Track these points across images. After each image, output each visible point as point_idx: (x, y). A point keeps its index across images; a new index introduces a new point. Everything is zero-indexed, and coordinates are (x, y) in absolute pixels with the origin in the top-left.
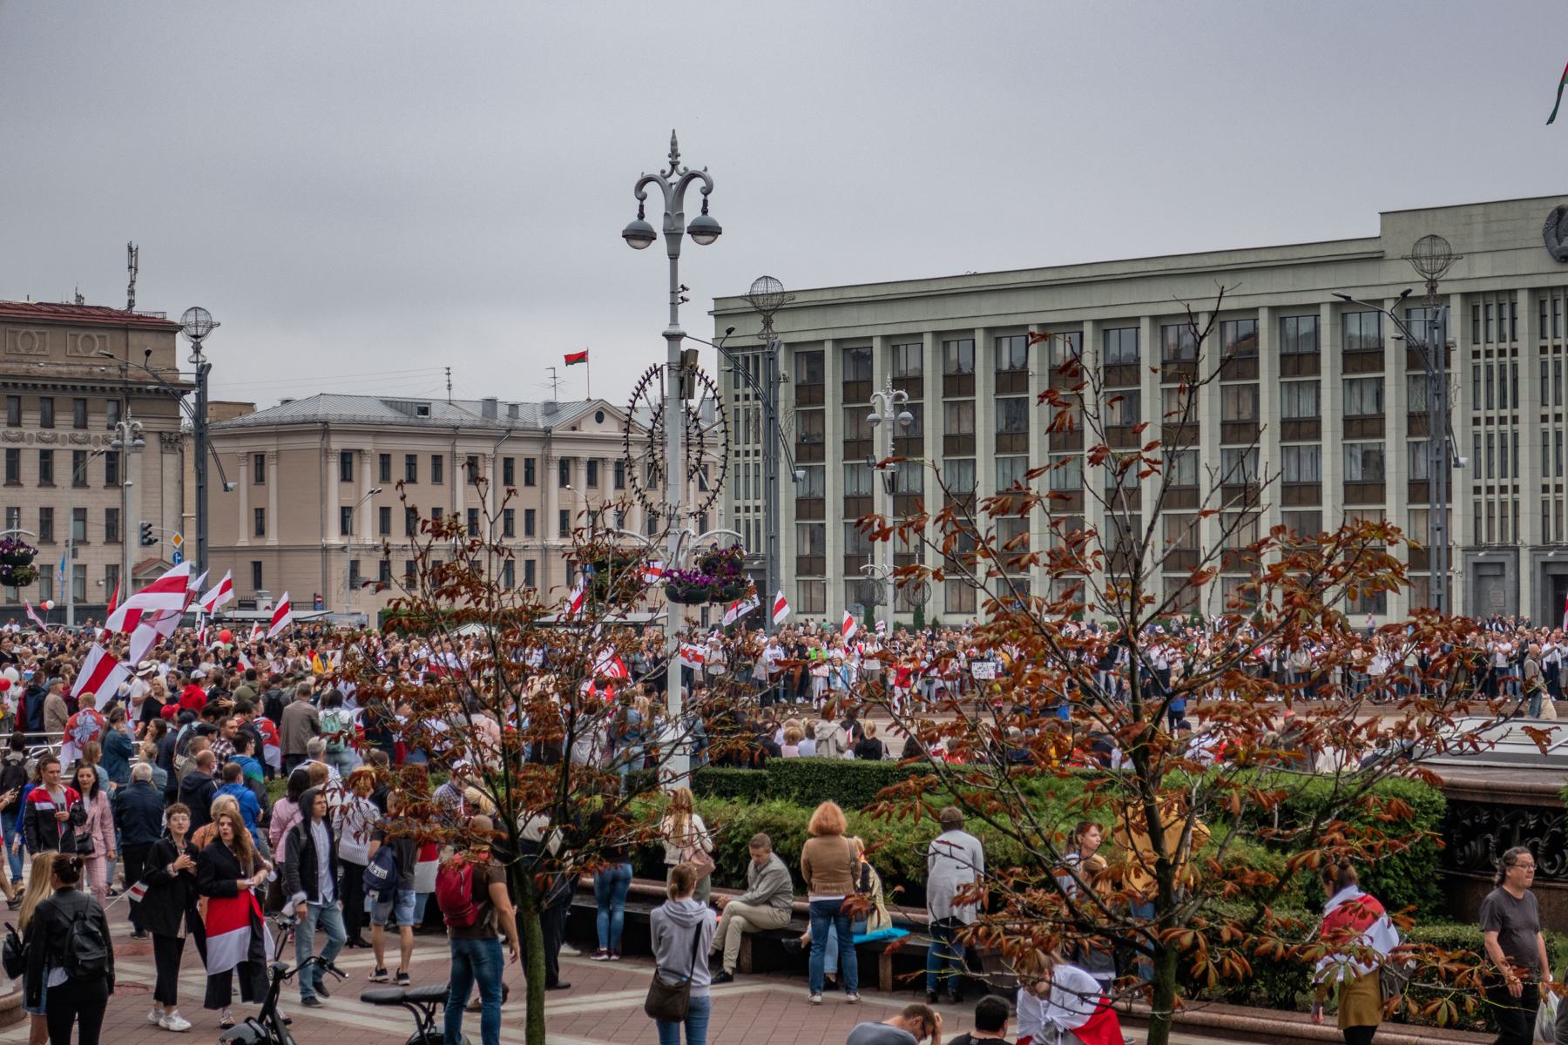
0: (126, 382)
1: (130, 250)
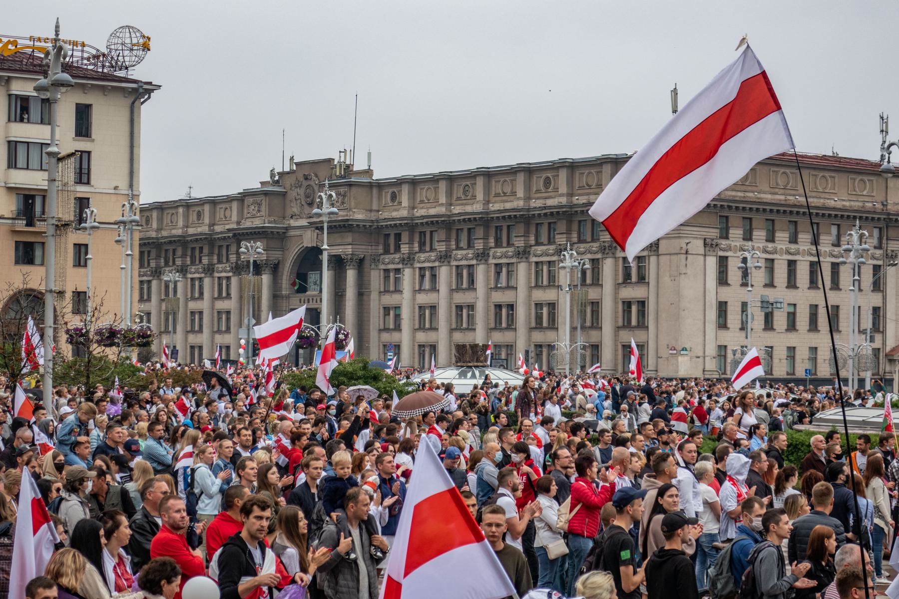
0: (889, 214)
1: (882, 118)
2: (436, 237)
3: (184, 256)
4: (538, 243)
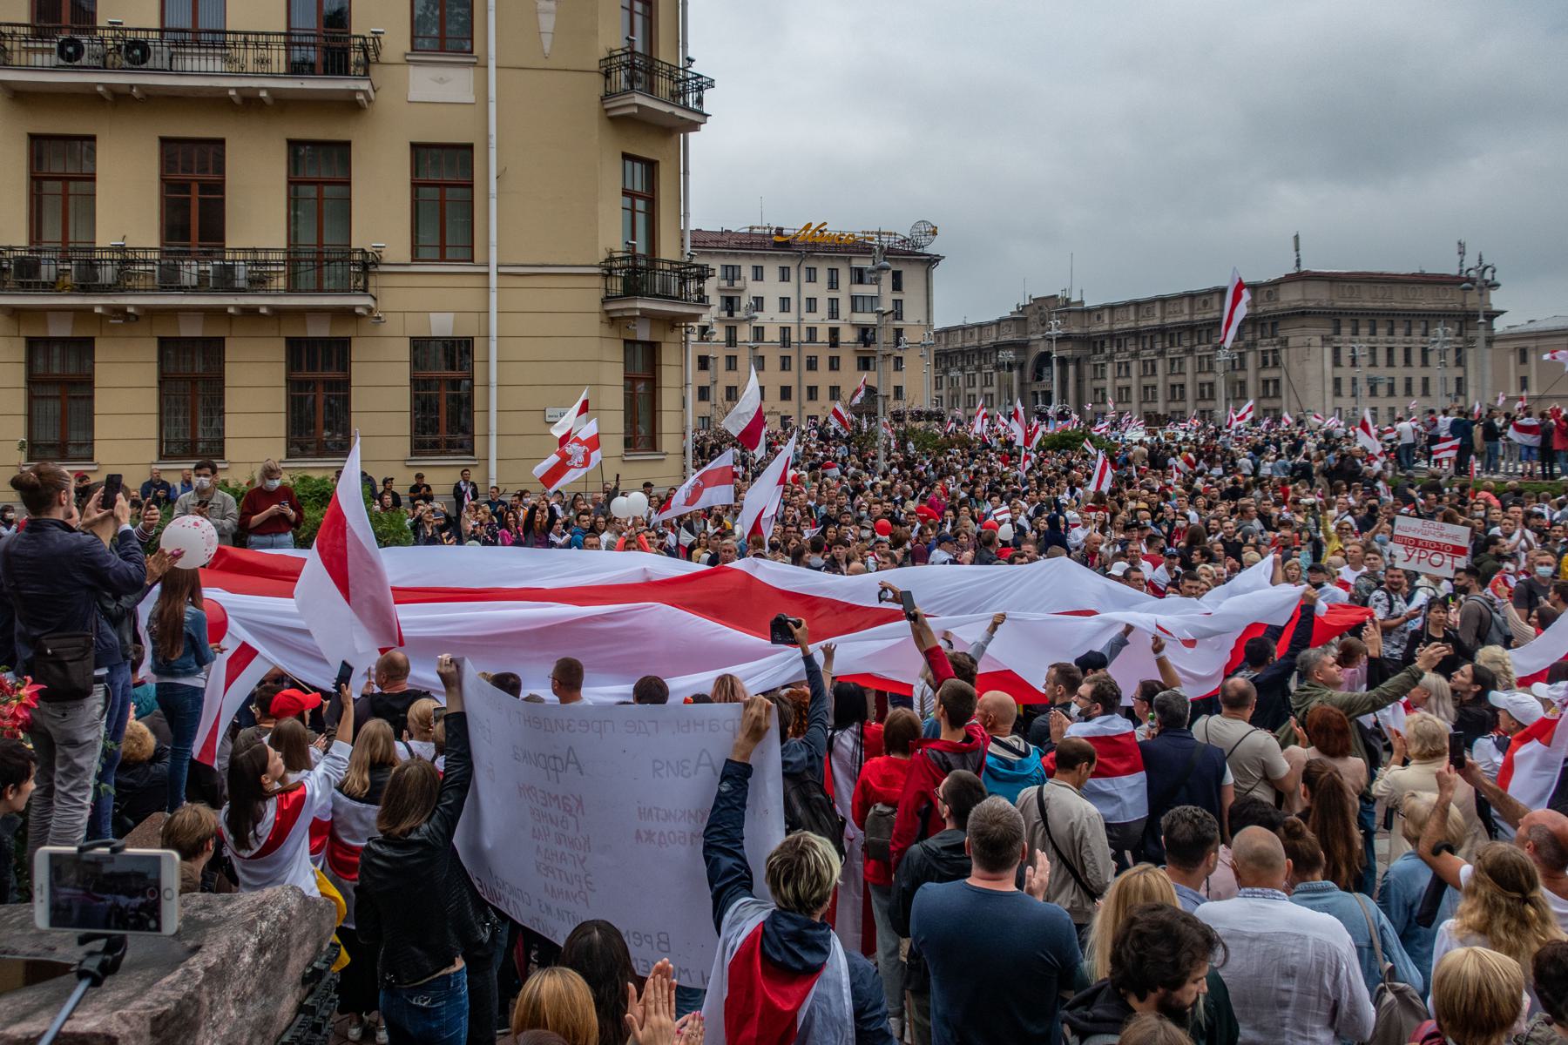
2: (1129, 342)
3: (963, 360)
4: (1200, 344)
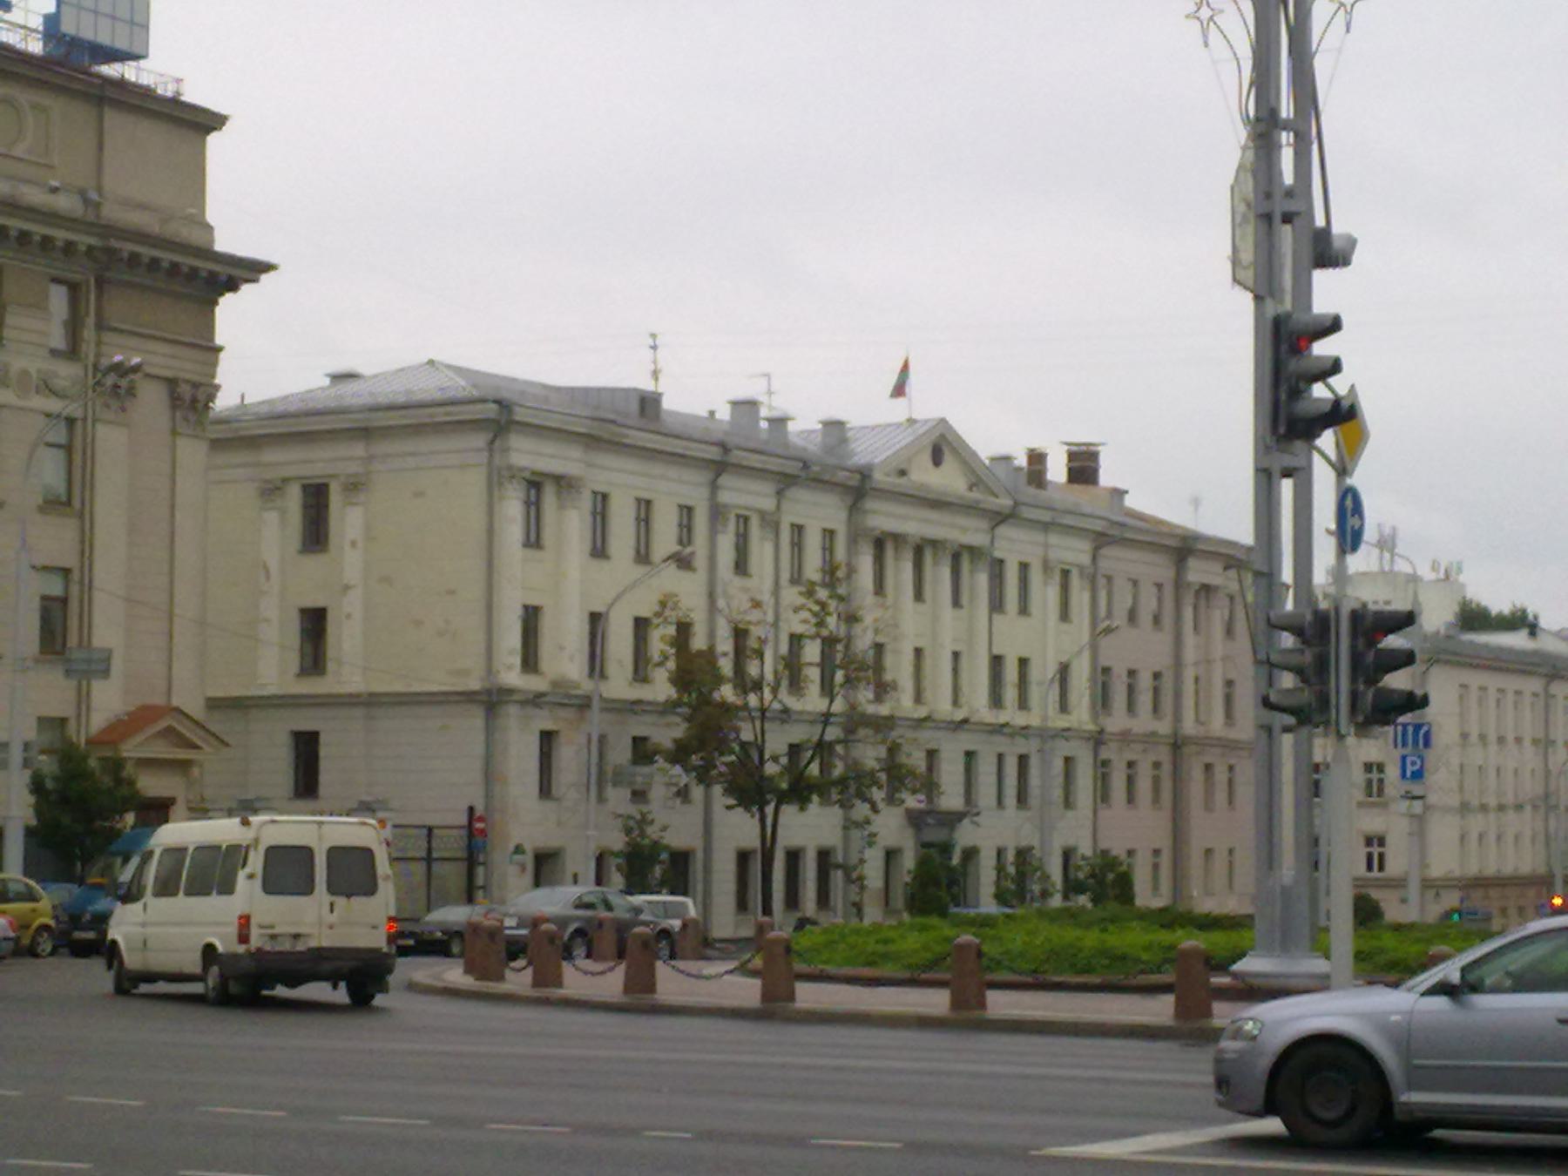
0: (109, 230)
